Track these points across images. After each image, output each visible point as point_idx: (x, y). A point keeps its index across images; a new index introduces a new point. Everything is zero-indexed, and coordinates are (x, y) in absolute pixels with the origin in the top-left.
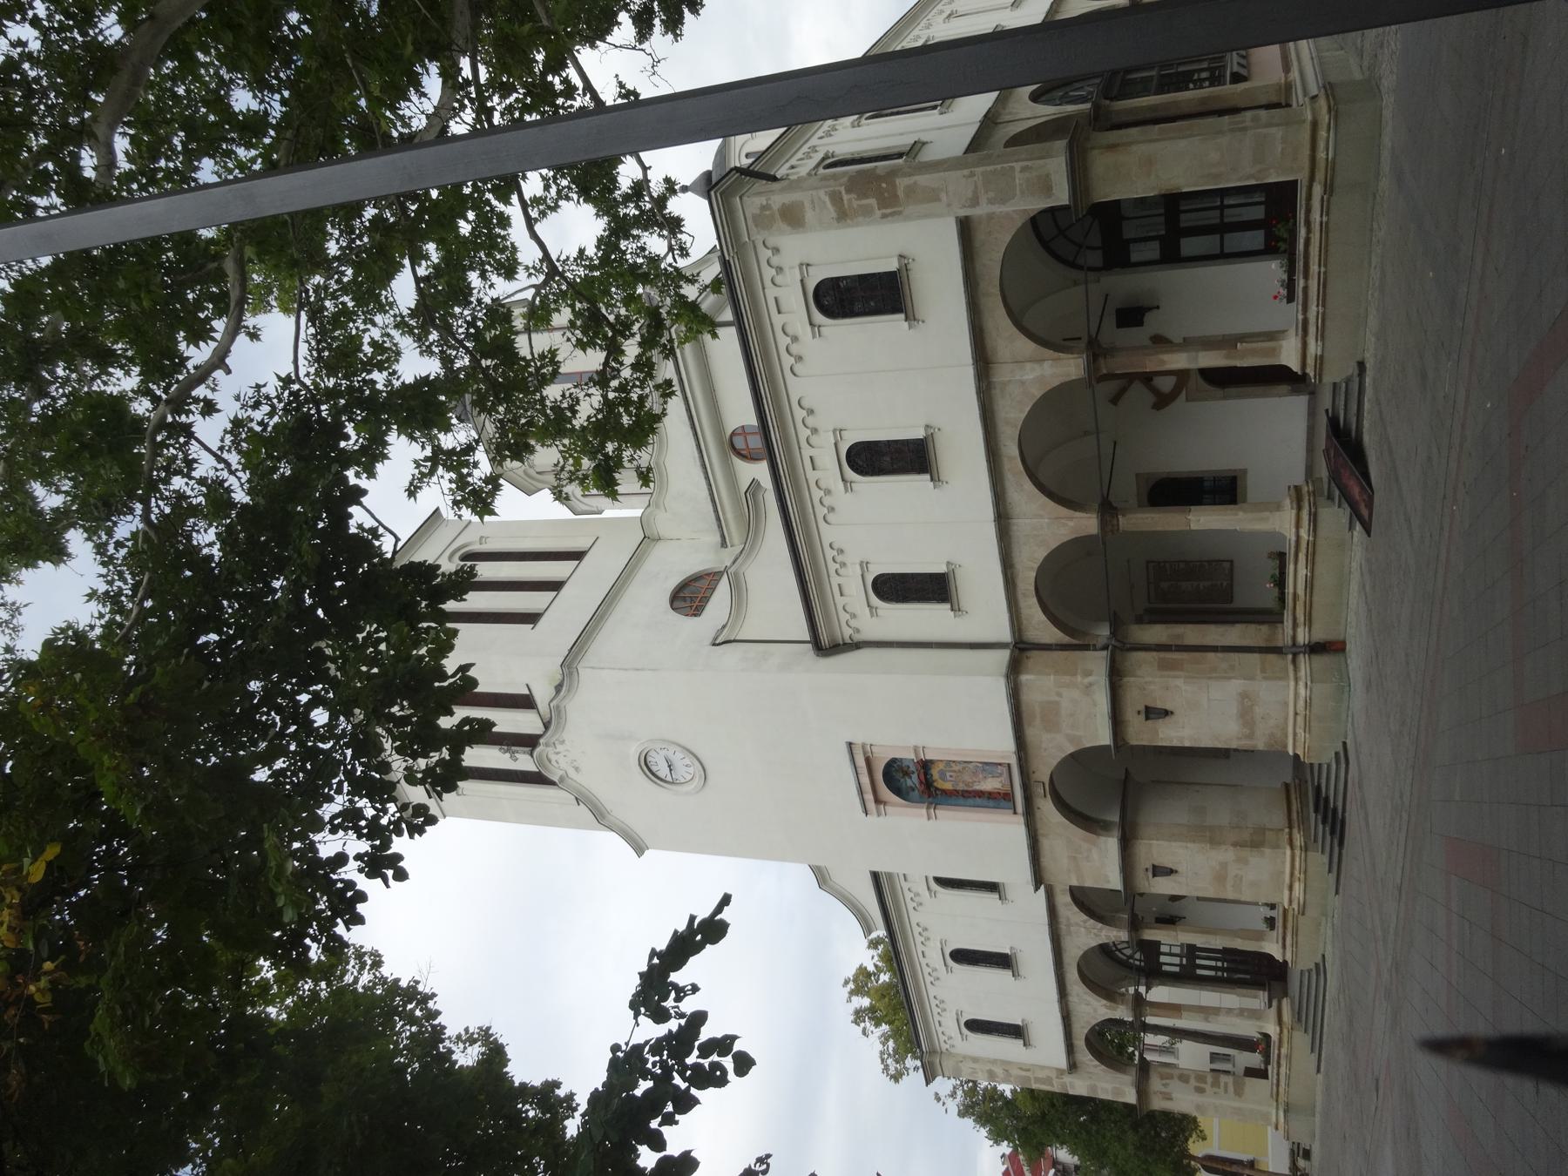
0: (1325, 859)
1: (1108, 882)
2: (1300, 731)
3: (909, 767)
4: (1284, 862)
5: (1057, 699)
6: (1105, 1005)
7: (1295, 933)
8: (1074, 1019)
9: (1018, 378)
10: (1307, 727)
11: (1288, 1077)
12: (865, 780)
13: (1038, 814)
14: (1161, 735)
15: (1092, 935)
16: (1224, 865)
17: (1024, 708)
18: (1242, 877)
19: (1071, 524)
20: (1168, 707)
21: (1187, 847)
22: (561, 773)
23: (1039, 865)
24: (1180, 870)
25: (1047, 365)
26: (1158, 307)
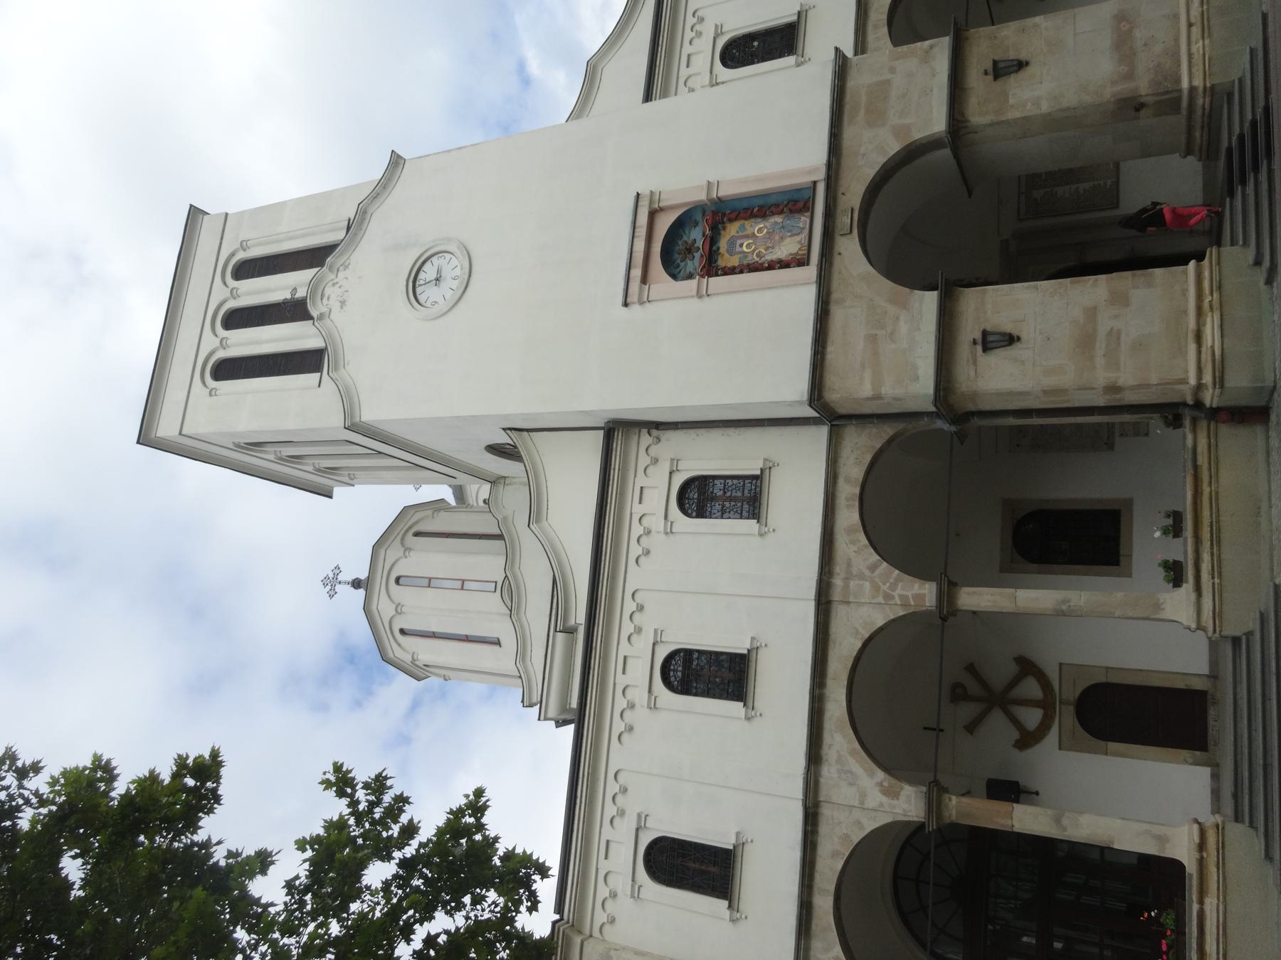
0: (1251, 253)
2: (1197, 47)
4: (1185, 292)
5: (889, 76)
6: (880, 784)
7: (1217, 540)
8: (823, 829)
10: (1206, 31)
11: (1223, 929)
12: (640, 246)
13: (837, 261)
14: (1012, 101)
15: (880, 599)
16: (1092, 313)
17: (848, 97)
18: (1119, 332)
20: (1023, 56)
22: (324, 310)
23: (823, 359)
24: (1024, 336)
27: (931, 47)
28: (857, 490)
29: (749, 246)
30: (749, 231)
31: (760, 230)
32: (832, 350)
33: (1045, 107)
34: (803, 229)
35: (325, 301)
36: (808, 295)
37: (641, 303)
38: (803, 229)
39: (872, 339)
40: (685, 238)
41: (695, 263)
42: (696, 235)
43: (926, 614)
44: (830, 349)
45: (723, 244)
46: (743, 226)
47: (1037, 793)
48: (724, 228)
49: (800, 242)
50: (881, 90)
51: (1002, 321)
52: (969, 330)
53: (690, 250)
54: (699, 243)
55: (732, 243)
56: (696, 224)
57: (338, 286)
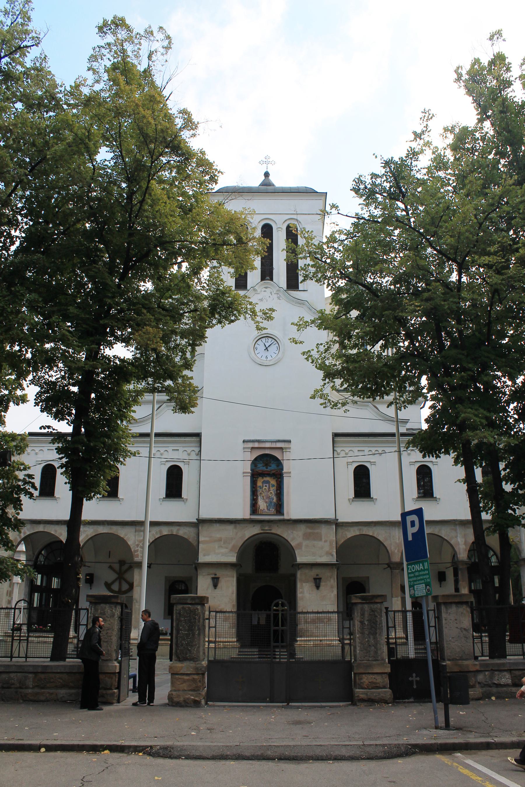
1: (204, 555)
3: (270, 466)
5: (323, 540)
9: (459, 535)
10: (315, 646)
12: (268, 445)
13: (251, 525)
14: (304, 584)
15: (137, 543)
17: (317, 525)
19: (396, 551)
20: (321, 588)
21: (233, 593)
23: (214, 523)
24: (217, 590)
25: (464, 546)
26: (441, 587)
27: (332, 555)
28: (174, 533)
29: (265, 489)
30: (271, 489)
31: (271, 493)
32: (217, 526)
33: (299, 595)
34: (269, 510)
35: (265, 289)
36: (239, 515)
37: (244, 448)
38: (269, 510)
39: (220, 540)
40: (272, 462)
41: (261, 467)
42: (273, 467)
43: (133, 559)
44: (218, 525)
45: (268, 479)
46: (273, 486)
47: (91, 589)
48: (274, 479)
49: (264, 509)
50: (318, 537)
51: (222, 583)
52: (220, 573)
53: (267, 465)
54: (269, 468)
55: (268, 482)
56: (278, 466)
57: (270, 295)
